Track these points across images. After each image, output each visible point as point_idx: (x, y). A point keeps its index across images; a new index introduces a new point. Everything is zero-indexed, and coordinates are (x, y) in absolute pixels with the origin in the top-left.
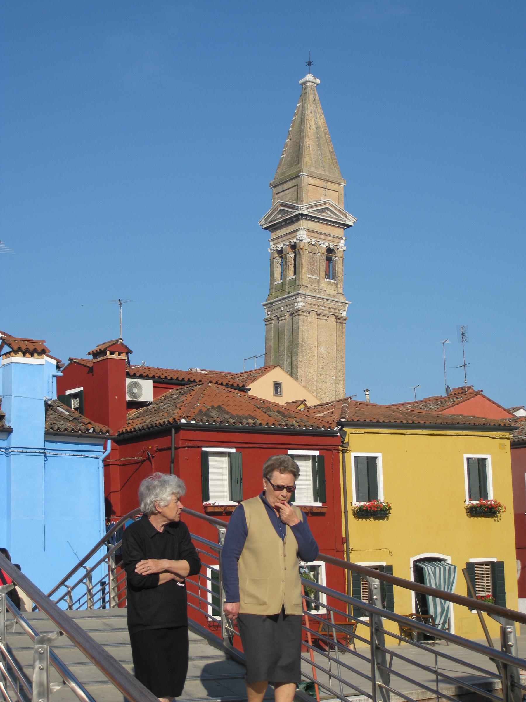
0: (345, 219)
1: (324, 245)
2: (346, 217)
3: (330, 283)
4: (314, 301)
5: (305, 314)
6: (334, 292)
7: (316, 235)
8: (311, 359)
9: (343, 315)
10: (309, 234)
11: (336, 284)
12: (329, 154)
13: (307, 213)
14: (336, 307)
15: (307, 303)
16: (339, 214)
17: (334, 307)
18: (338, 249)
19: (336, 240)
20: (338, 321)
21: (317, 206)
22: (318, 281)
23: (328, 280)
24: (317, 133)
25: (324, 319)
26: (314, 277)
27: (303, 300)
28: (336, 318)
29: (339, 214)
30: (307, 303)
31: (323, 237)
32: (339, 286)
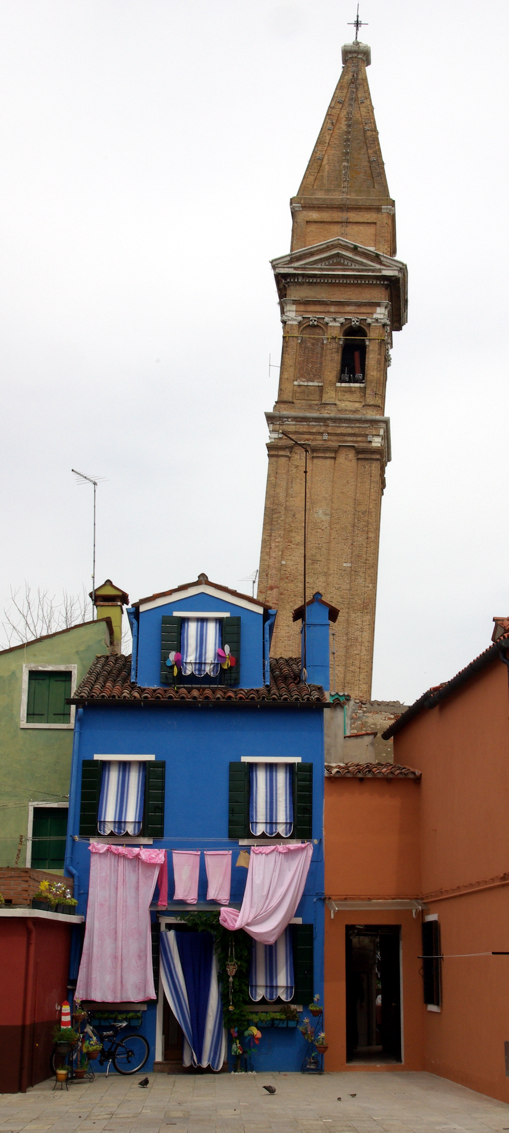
0: (378, 266)
2: (381, 263)
3: (350, 391)
4: (303, 427)
5: (281, 453)
6: (357, 405)
7: (318, 308)
8: (293, 534)
9: (374, 444)
10: (302, 308)
12: (366, 164)
14: (357, 431)
16: (365, 261)
17: (350, 431)
18: (369, 324)
19: (363, 310)
20: (360, 456)
21: (312, 254)
22: (321, 389)
23: (343, 385)
24: (348, 133)
25: (326, 458)
26: (311, 384)
27: (277, 427)
28: (359, 451)
29: (365, 261)
31: (332, 309)
32: (368, 391)
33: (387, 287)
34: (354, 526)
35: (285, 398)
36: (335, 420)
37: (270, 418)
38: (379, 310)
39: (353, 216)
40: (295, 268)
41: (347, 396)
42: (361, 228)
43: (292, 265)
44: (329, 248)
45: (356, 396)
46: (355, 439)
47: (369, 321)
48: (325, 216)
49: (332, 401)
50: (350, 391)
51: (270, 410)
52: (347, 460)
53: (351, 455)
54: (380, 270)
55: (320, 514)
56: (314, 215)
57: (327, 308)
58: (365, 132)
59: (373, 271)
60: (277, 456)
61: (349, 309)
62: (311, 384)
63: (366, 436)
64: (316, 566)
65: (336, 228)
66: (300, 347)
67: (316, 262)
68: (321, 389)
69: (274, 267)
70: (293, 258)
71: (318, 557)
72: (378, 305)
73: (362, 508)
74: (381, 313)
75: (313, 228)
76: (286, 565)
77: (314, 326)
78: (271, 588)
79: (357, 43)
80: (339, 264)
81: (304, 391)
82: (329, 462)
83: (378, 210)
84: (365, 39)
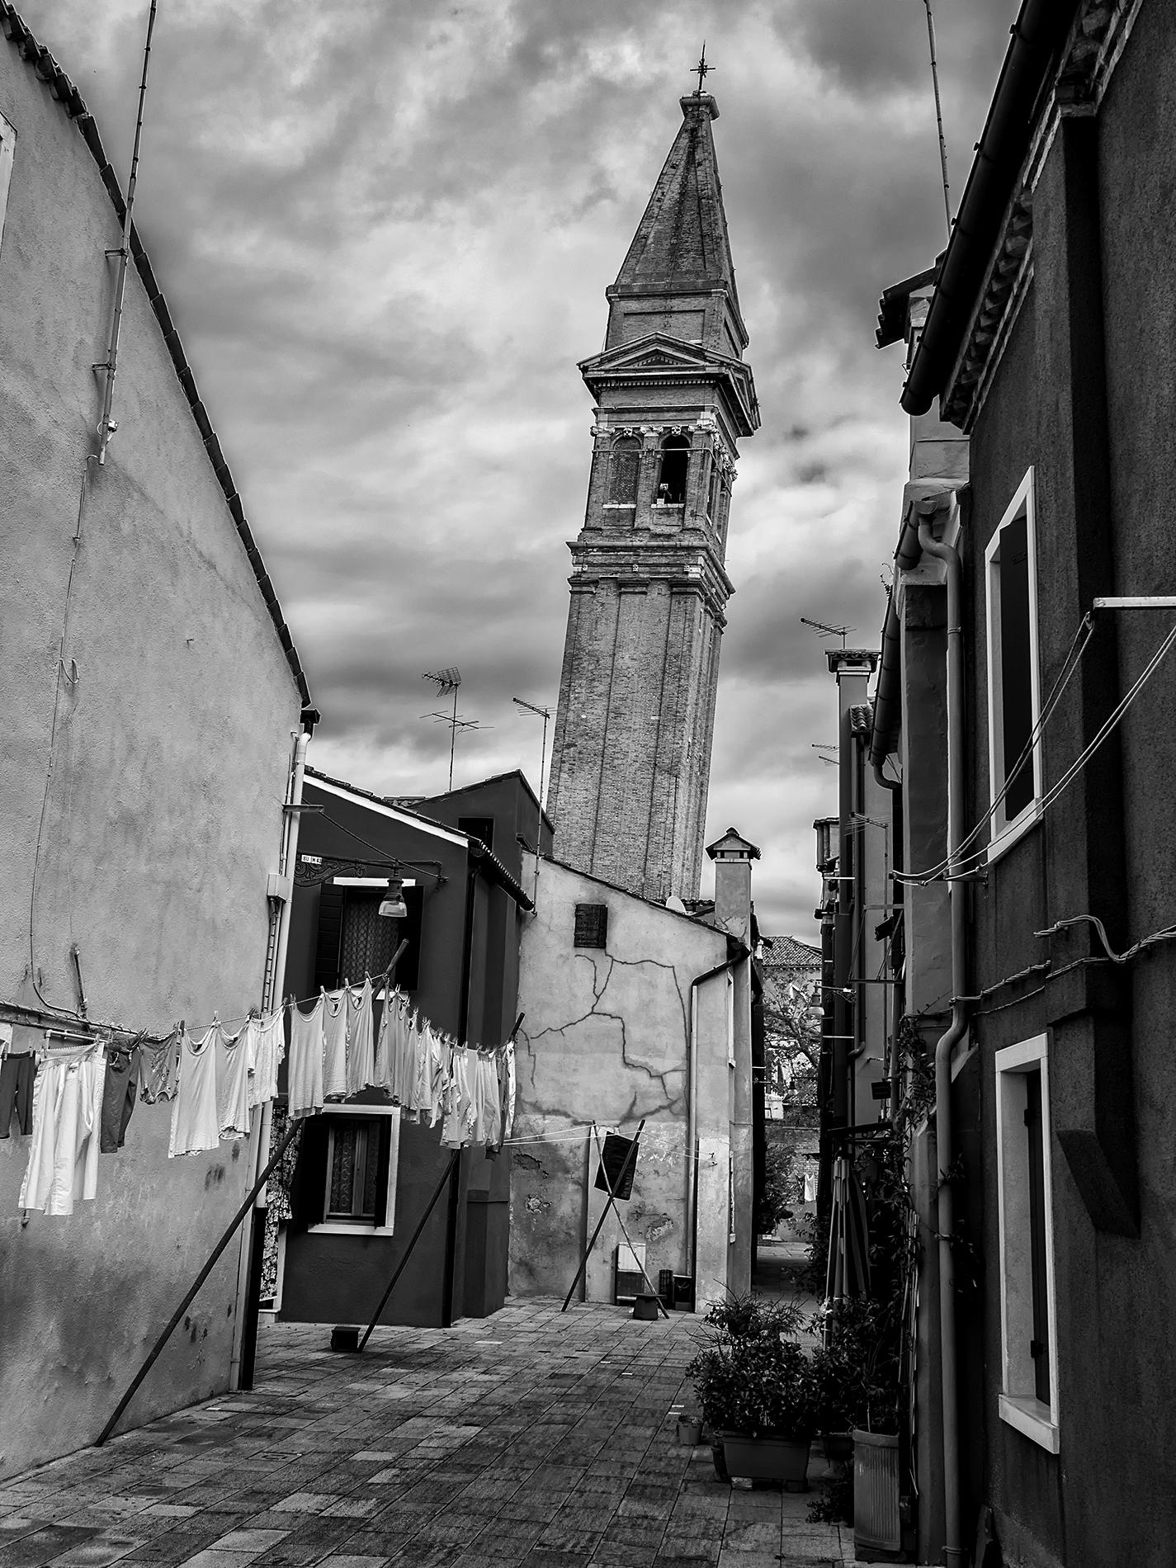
0: (702, 363)
1: (651, 432)
4: (610, 558)
5: (585, 589)
7: (633, 416)
10: (615, 417)
11: (682, 511)
13: (603, 374)
15: (591, 565)
17: (664, 560)
19: (686, 415)
21: (626, 353)
22: (634, 512)
30: (591, 565)
31: (650, 416)
32: (688, 513)
33: (714, 387)
34: (664, 672)
35: (592, 524)
36: (647, 548)
37: (574, 548)
38: (706, 414)
39: (676, 304)
40: (606, 371)
41: (664, 519)
42: (687, 316)
43: (608, 366)
44: (644, 345)
45: (675, 519)
46: (668, 569)
47: (691, 428)
48: (646, 305)
49: (645, 525)
50: (667, 513)
51: (574, 539)
52: (658, 596)
53: (664, 589)
54: (704, 368)
55: (625, 660)
56: (634, 306)
57: (644, 416)
58: (700, 199)
59: (695, 369)
60: (581, 593)
61: (668, 415)
62: (622, 506)
63: (682, 565)
64: (619, 720)
65: (657, 319)
66: (617, 460)
67: (631, 362)
68: (634, 512)
69: (585, 370)
70: (604, 359)
71: (623, 710)
72: (702, 409)
73: (673, 651)
74: (707, 419)
75: (632, 320)
76: (586, 720)
77: (628, 438)
78: (569, 746)
79: (697, 95)
80: (660, 362)
81: (615, 517)
82: (637, 598)
83: (708, 294)
84: (710, 88)
